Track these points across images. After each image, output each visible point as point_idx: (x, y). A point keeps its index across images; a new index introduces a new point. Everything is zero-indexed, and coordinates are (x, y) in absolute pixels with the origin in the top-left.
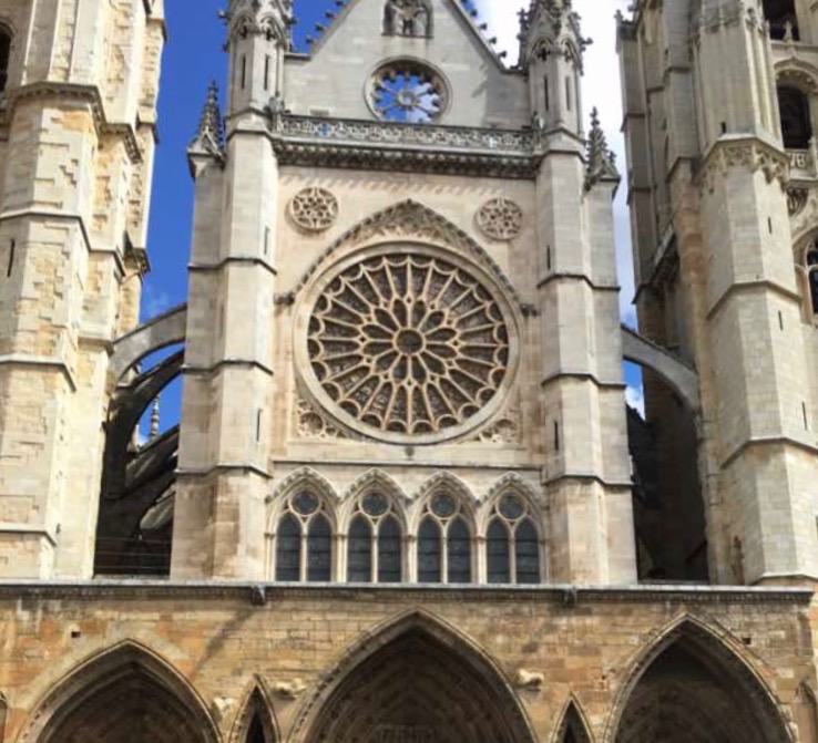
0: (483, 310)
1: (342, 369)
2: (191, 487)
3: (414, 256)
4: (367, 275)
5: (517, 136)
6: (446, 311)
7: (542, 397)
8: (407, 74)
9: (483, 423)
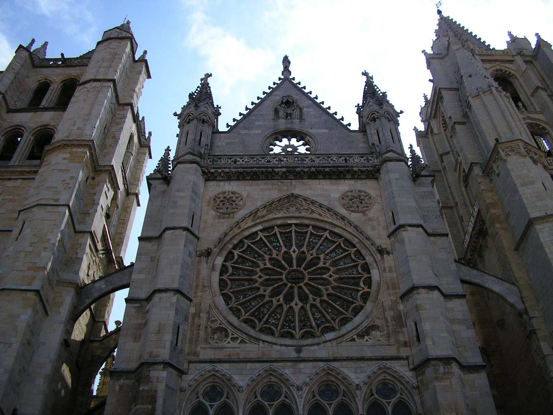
0: (350, 254)
1: (244, 298)
2: (122, 381)
3: (296, 225)
4: (263, 238)
5: (362, 157)
6: (322, 256)
7: (401, 307)
9: (356, 328)
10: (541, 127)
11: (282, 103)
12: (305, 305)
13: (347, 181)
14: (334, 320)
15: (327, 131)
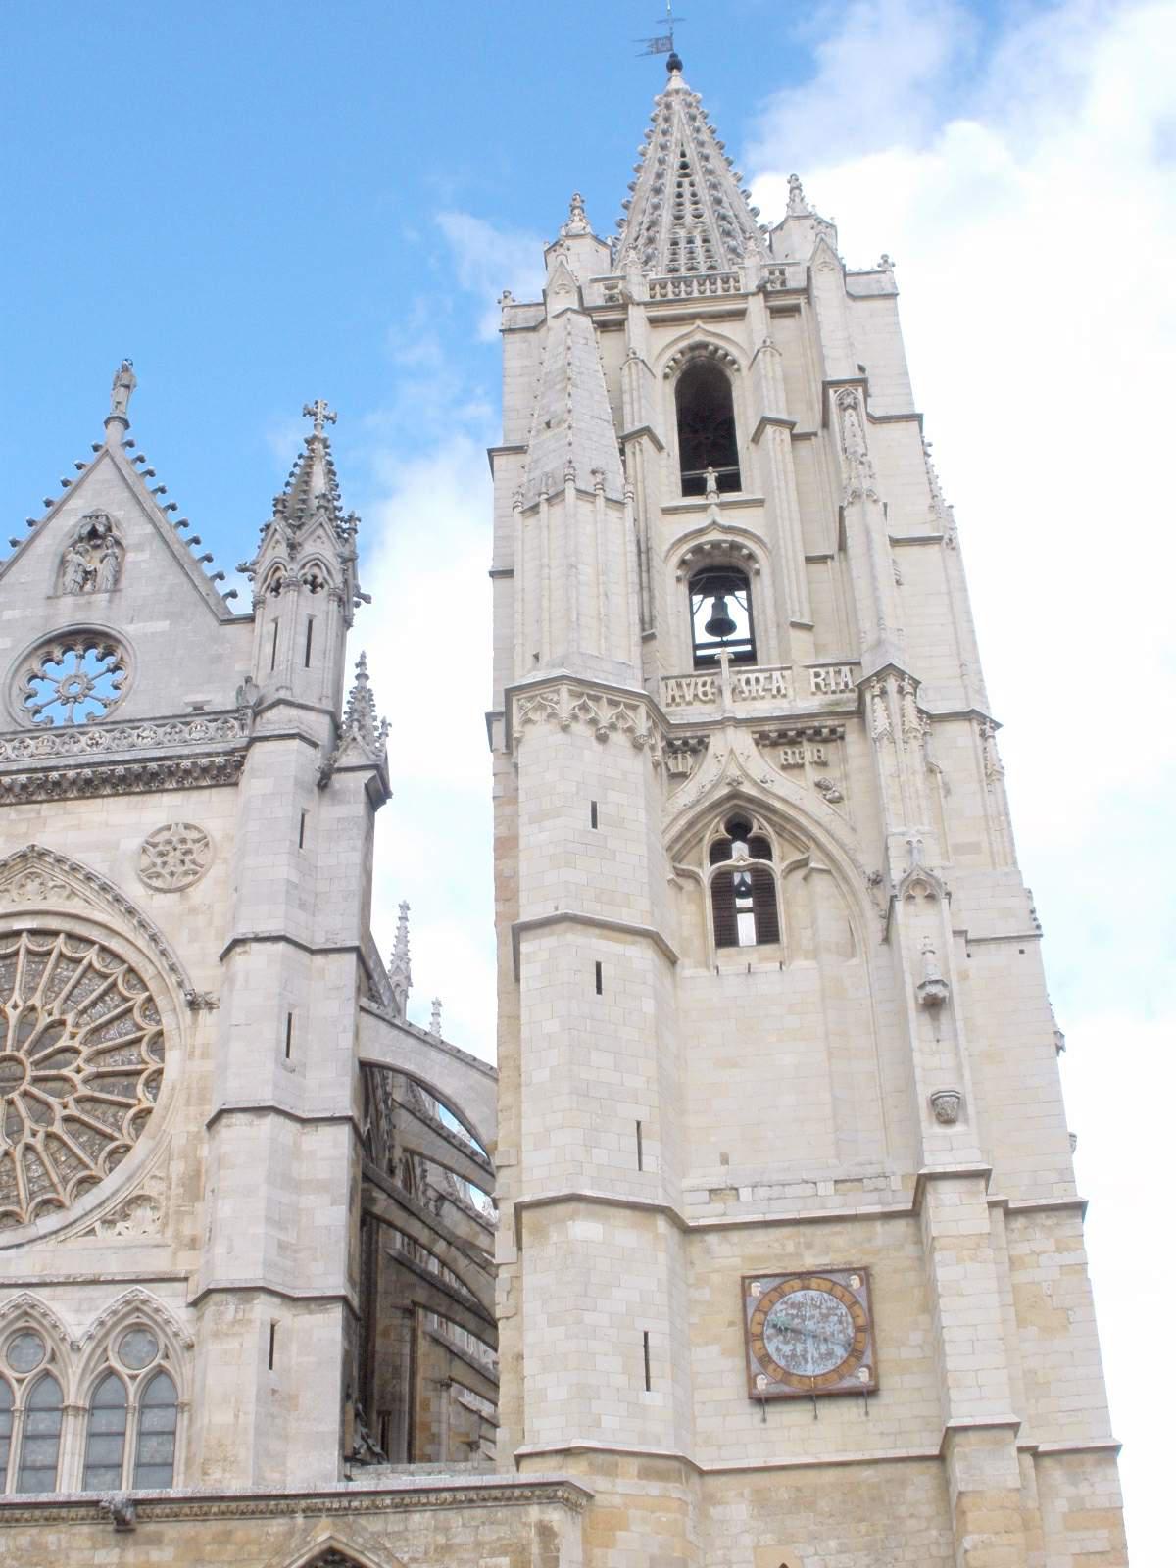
0: (130, 1010)
3: (33, 932)
6: (70, 1018)
8: (80, 649)
9: (100, 1206)
10: (745, 551)
11: (81, 539)
12: (11, 1150)
13: (166, 798)
14: (65, 1180)
15: (163, 625)
